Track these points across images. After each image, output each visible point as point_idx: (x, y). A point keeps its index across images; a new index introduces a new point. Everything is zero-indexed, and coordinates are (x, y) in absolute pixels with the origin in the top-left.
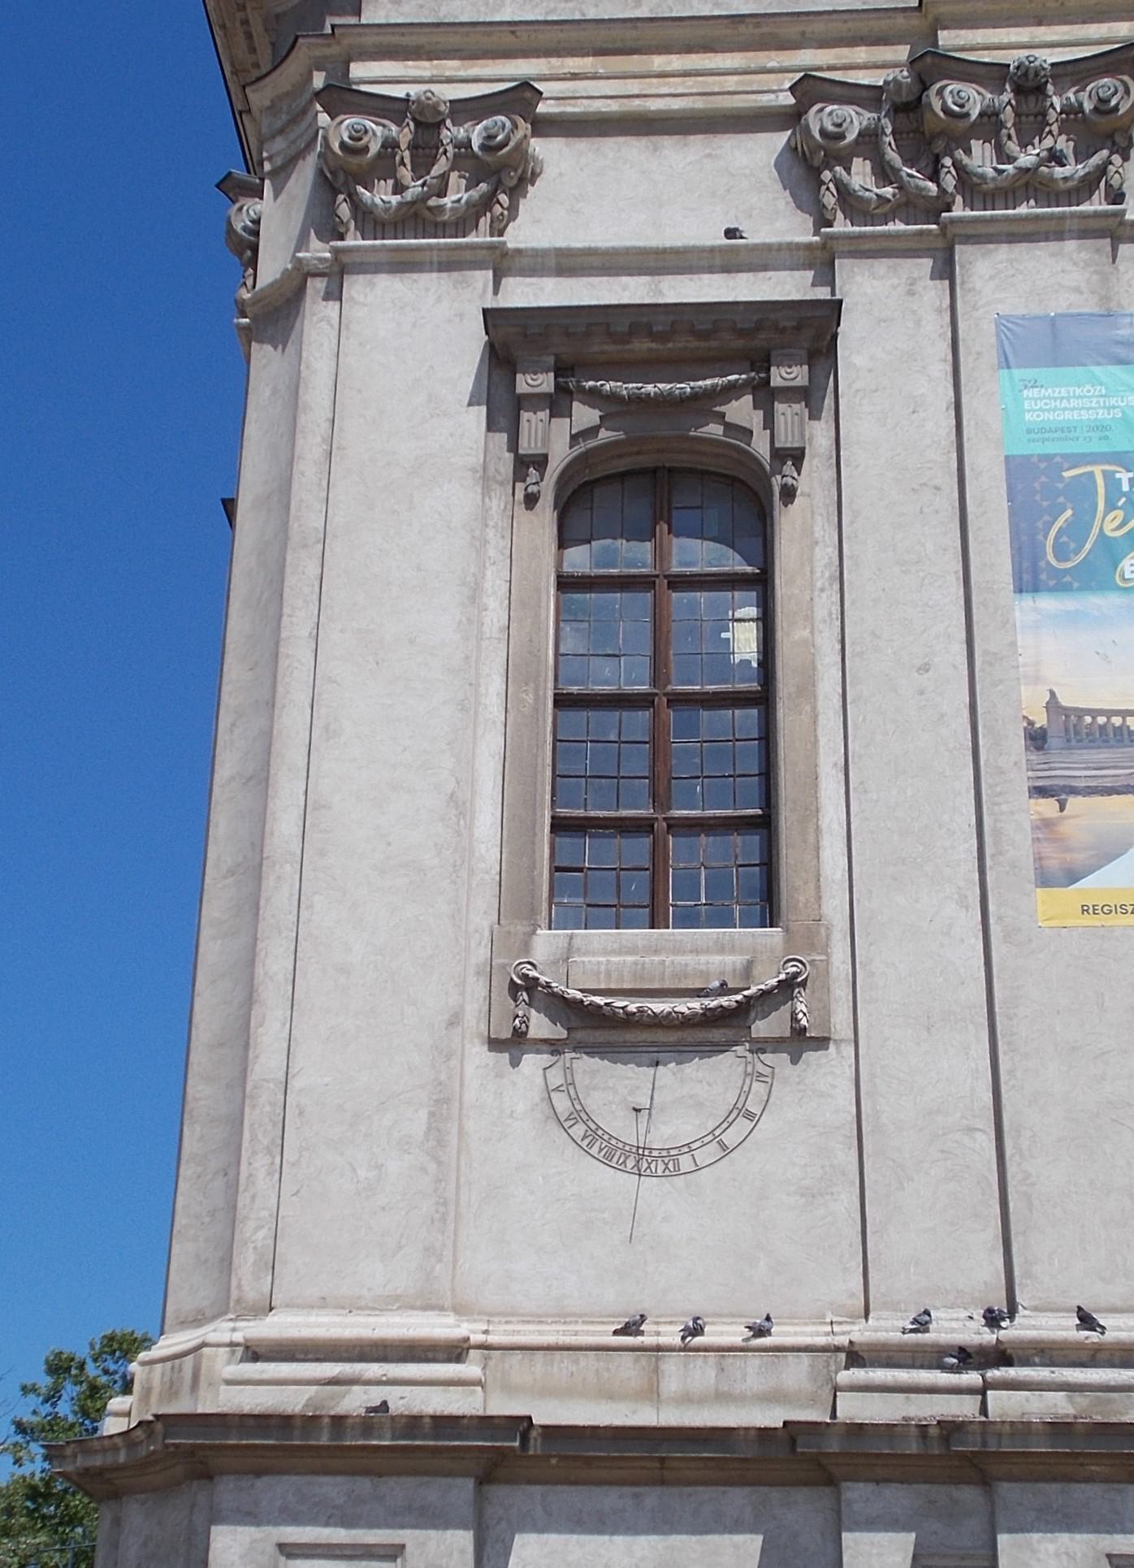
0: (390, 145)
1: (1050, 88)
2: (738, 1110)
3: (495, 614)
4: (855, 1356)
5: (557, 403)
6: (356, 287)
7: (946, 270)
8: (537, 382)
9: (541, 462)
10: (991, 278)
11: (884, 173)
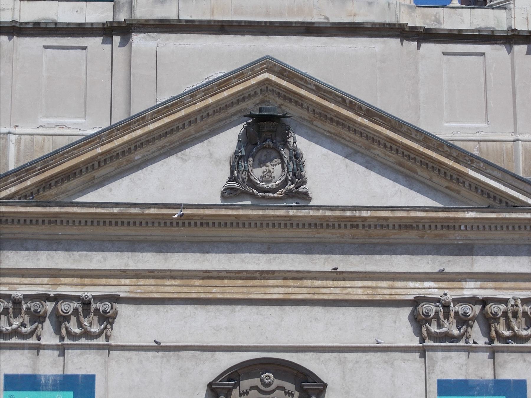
1: (23, 302)
10: (4, 361)
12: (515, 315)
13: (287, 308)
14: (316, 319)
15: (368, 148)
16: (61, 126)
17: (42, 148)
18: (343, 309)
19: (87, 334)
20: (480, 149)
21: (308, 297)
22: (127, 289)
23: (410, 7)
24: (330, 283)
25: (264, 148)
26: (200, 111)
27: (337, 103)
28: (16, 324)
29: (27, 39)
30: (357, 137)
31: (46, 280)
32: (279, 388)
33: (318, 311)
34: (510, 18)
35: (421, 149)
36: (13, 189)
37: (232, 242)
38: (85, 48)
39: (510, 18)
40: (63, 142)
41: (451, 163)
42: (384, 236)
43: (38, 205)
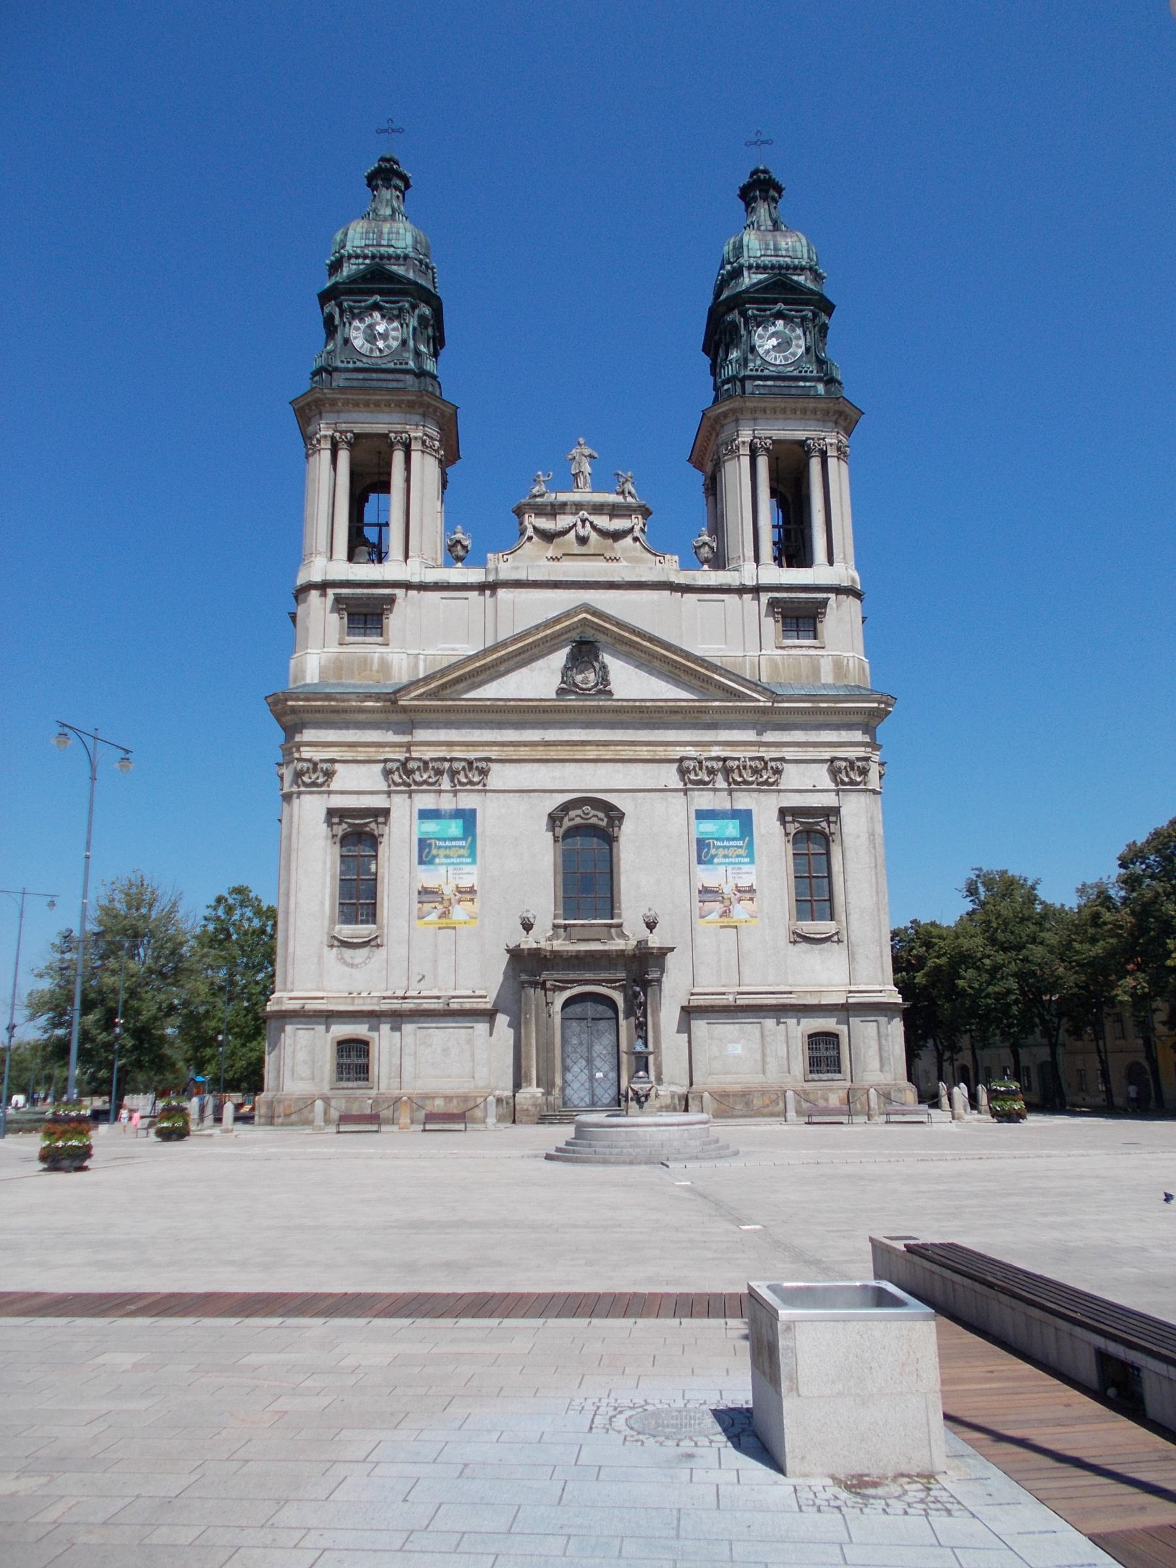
0: (308, 768)
2: (369, 957)
3: (328, 866)
4: (384, 998)
5: (339, 824)
6: (302, 797)
7: (410, 797)
8: (336, 820)
9: (336, 836)
11: (401, 777)
12: (745, 768)
13: (599, 764)
14: (618, 772)
15: (650, 662)
16: (453, 649)
17: (441, 664)
18: (635, 765)
19: (471, 783)
20: (721, 662)
21: (613, 757)
22: (496, 753)
23: (676, 570)
24: (627, 748)
25: (582, 662)
26: (541, 638)
27: (630, 633)
28: (425, 776)
29: (430, 593)
30: (643, 655)
31: (444, 748)
32: (594, 816)
33: (619, 766)
34: (741, 577)
35: (684, 662)
36: (422, 690)
37: (564, 723)
38: (467, 599)
39: (741, 577)
40: (454, 660)
41: (703, 671)
42: (660, 718)
43: (438, 700)
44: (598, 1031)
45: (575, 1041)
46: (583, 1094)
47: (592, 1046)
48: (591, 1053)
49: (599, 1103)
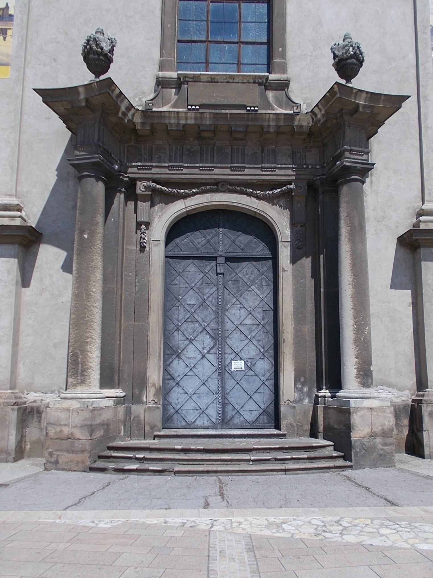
44: (236, 281)
45: (191, 299)
46: (204, 402)
47: (224, 310)
48: (223, 322)
49: (237, 420)
